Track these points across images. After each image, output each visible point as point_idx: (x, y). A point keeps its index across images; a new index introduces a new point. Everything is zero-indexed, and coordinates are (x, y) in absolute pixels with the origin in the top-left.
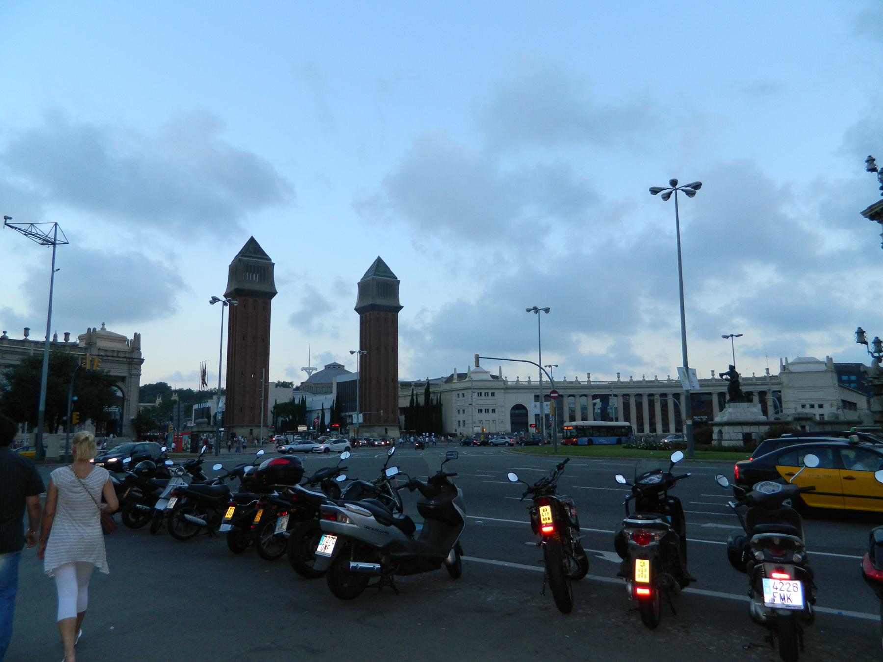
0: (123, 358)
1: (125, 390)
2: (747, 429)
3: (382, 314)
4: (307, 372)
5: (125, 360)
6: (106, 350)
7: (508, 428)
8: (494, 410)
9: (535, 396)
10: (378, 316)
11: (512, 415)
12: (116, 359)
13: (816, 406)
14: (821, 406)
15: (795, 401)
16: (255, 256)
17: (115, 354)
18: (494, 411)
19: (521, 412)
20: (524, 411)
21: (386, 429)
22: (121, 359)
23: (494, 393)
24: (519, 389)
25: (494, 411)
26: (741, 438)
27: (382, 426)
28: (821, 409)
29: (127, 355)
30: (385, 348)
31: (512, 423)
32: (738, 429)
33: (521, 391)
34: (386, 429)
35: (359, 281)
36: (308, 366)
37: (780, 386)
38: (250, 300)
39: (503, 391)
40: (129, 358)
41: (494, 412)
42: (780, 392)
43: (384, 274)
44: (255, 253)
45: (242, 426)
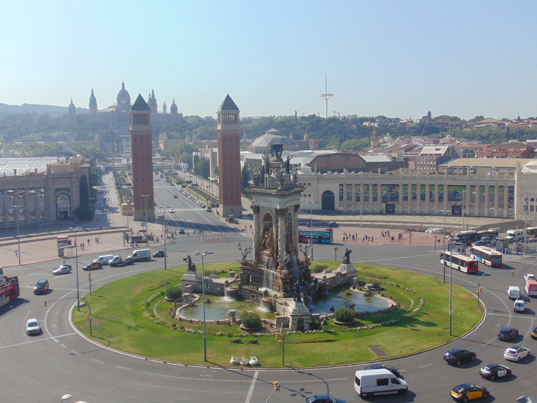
0: (68, 178)
2: (188, 283)
4: (324, 98)
5: (68, 179)
6: (57, 175)
7: (320, 207)
8: (310, 195)
9: (340, 185)
12: (63, 179)
17: (63, 176)
18: (310, 196)
19: (329, 195)
25: (310, 196)
26: (185, 285)
29: (70, 176)
32: (185, 282)
33: (329, 181)
36: (325, 93)
39: (316, 182)
40: (70, 178)
41: (310, 196)
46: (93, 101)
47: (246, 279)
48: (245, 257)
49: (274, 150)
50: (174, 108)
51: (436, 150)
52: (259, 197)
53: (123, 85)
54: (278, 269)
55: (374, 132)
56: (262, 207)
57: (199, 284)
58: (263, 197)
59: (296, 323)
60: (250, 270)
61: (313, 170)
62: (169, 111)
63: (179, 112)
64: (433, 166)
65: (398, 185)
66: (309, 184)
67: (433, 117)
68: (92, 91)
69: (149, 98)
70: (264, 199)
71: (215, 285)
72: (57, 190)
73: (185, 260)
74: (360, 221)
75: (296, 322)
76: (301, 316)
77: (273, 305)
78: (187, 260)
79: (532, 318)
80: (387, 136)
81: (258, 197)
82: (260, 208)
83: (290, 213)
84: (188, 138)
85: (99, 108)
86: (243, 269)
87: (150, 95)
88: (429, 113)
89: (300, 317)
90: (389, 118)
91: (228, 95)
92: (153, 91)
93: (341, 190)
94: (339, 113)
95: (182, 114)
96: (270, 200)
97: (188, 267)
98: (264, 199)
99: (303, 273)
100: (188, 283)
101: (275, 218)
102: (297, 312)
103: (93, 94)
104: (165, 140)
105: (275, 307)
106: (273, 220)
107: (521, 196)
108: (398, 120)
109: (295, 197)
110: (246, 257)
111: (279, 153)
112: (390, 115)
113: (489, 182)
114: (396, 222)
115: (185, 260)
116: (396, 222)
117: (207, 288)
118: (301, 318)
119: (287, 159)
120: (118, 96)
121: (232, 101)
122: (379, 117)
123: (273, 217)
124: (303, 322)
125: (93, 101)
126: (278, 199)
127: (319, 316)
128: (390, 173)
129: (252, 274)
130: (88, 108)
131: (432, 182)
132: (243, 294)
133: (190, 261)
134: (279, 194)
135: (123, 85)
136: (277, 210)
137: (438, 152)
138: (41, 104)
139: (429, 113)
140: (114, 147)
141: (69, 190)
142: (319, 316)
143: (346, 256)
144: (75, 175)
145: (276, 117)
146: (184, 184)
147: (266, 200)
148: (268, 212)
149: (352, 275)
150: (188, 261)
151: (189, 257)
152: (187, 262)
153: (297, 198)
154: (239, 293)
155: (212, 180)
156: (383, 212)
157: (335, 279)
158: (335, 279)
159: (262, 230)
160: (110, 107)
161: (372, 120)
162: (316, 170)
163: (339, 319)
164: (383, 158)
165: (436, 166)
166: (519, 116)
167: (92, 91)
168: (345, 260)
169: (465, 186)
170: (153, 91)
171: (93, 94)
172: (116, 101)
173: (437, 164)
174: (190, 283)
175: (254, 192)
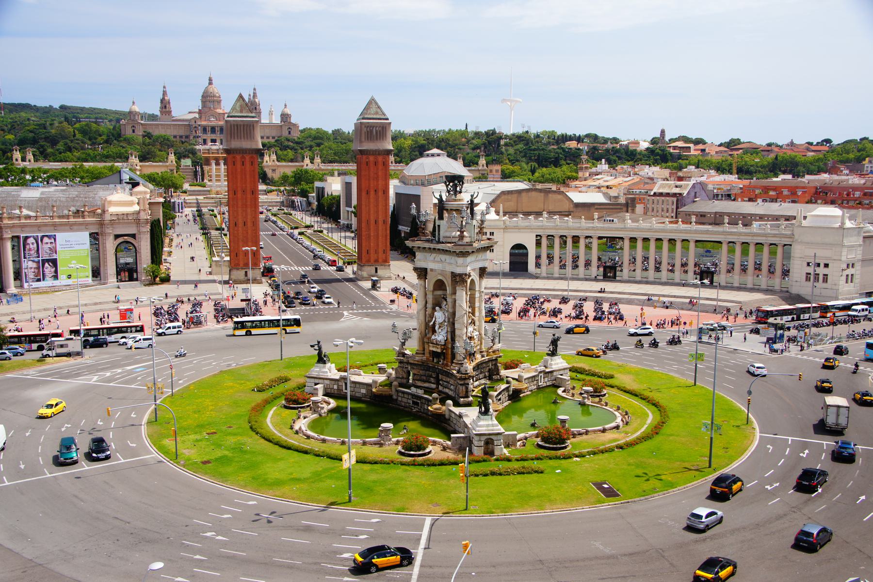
1: (136, 245)
2: (317, 381)
3: (372, 158)
7: (507, 268)
9: (537, 236)
10: (367, 160)
11: (511, 255)
13: (822, 265)
14: (826, 266)
15: (801, 258)
16: (240, 115)
19: (521, 251)
20: (525, 251)
21: (376, 269)
22: (130, 221)
23: (493, 233)
24: (519, 229)
26: (313, 384)
27: (373, 266)
28: (826, 269)
29: (135, 216)
30: (376, 191)
31: (511, 263)
32: (313, 380)
33: (522, 230)
34: (376, 269)
35: (356, 122)
37: (791, 240)
38: (238, 157)
41: (493, 251)
42: (791, 245)
43: (375, 116)
44: (241, 111)
45: (238, 269)
46: (165, 105)
47: (405, 376)
48: (403, 344)
49: (451, 184)
50: (285, 117)
51: (676, 187)
52: (427, 255)
53: (210, 79)
54: (452, 362)
55: (584, 157)
56: (432, 270)
57: (333, 382)
58: (434, 255)
59: (483, 445)
60: (411, 364)
61: (497, 213)
62: (277, 120)
63: (293, 120)
64: (670, 210)
65: (622, 238)
66: (491, 233)
67: (667, 139)
68: (164, 87)
69: (249, 99)
70: (434, 258)
71: (358, 386)
72: (117, 237)
73: (312, 346)
74: (566, 290)
75: (482, 443)
76: (490, 434)
77: (447, 417)
78: (316, 347)
79: (825, 443)
80: (601, 164)
81: (426, 254)
82: (428, 270)
83: (472, 280)
84: (307, 161)
85: (174, 114)
86: (401, 362)
87: (250, 95)
88: (663, 132)
89: (488, 437)
90: (603, 137)
91: (372, 97)
92: (255, 89)
93: (538, 243)
94: (529, 127)
95: (295, 125)
96: (443, 260)
97: (317, 358)
98: (434, 258)
99: (489, 369)
100: (317, 381)
101: (450, 287)
102: (485, 428)
103: (165, 93)
104: (273, 163)
105: (449, 420)
106: (448, 288)
107: (802, 259)
108: (615, 140)
109: (481, 256)
110: (404, 345)
111: (458, 189)
112: (604, 132)
113: (755, 238)
114: (619, 293)
115: (312, 346)
116: (619, 293)
117: (346, 389)
118: (490, 439)
119: (470, 198)
120: (203, 96)
121: (379, 107)
122: (588, 136)
123: (447, 285)
124: (493, 444)
125: (165, 105)
126: (456, 258)
127: (516, 435)
128: (610, 220)
129: (414, 369)
130: (157, 113)
131: (672, 236)
132: (400, 399)
133: (320, 349)
134: (458, 251)
135: (210, 79)
136: (454, 275)
137: (677, 191)
138: (87, 106)
139: (663, 132)
140: (196, 172)
141: (133, 236)
142: (516, 435)
143: (553, 345)
144: (144, 216)
145: (437, 130)
146: (303, 230)
147: (438, 259)
148: (440, 278)
149: (561, 372)
150: (317, 348)
151: (319, 342)
152: (316, 350)
153: (483, 258)
154: (395, 397)
155: (344, 224)
156: (598, 277)
157: (537, 379)
158: (537, 379)
159: (429, 306)
160: (190, 113)
161: (579, 139)
162: (501, 213)
163: (543, 440)
164: (598, 198)
165: (675, 210)
166: (792, 140)
167: (164, 87)
168: (550, 351)
169: (720, 242)
170: (255, 89)
171: (165, 93)
172: (200, 104)
173: (677, 208)
174: (320, 381)
175: (419, 247)
